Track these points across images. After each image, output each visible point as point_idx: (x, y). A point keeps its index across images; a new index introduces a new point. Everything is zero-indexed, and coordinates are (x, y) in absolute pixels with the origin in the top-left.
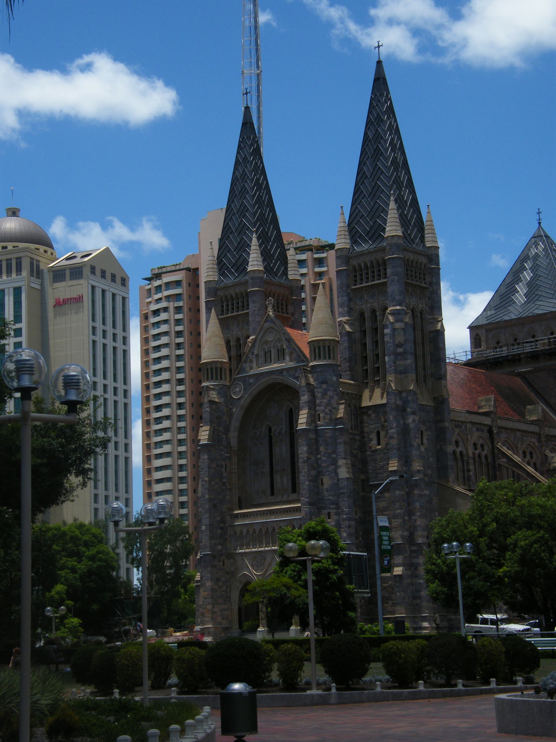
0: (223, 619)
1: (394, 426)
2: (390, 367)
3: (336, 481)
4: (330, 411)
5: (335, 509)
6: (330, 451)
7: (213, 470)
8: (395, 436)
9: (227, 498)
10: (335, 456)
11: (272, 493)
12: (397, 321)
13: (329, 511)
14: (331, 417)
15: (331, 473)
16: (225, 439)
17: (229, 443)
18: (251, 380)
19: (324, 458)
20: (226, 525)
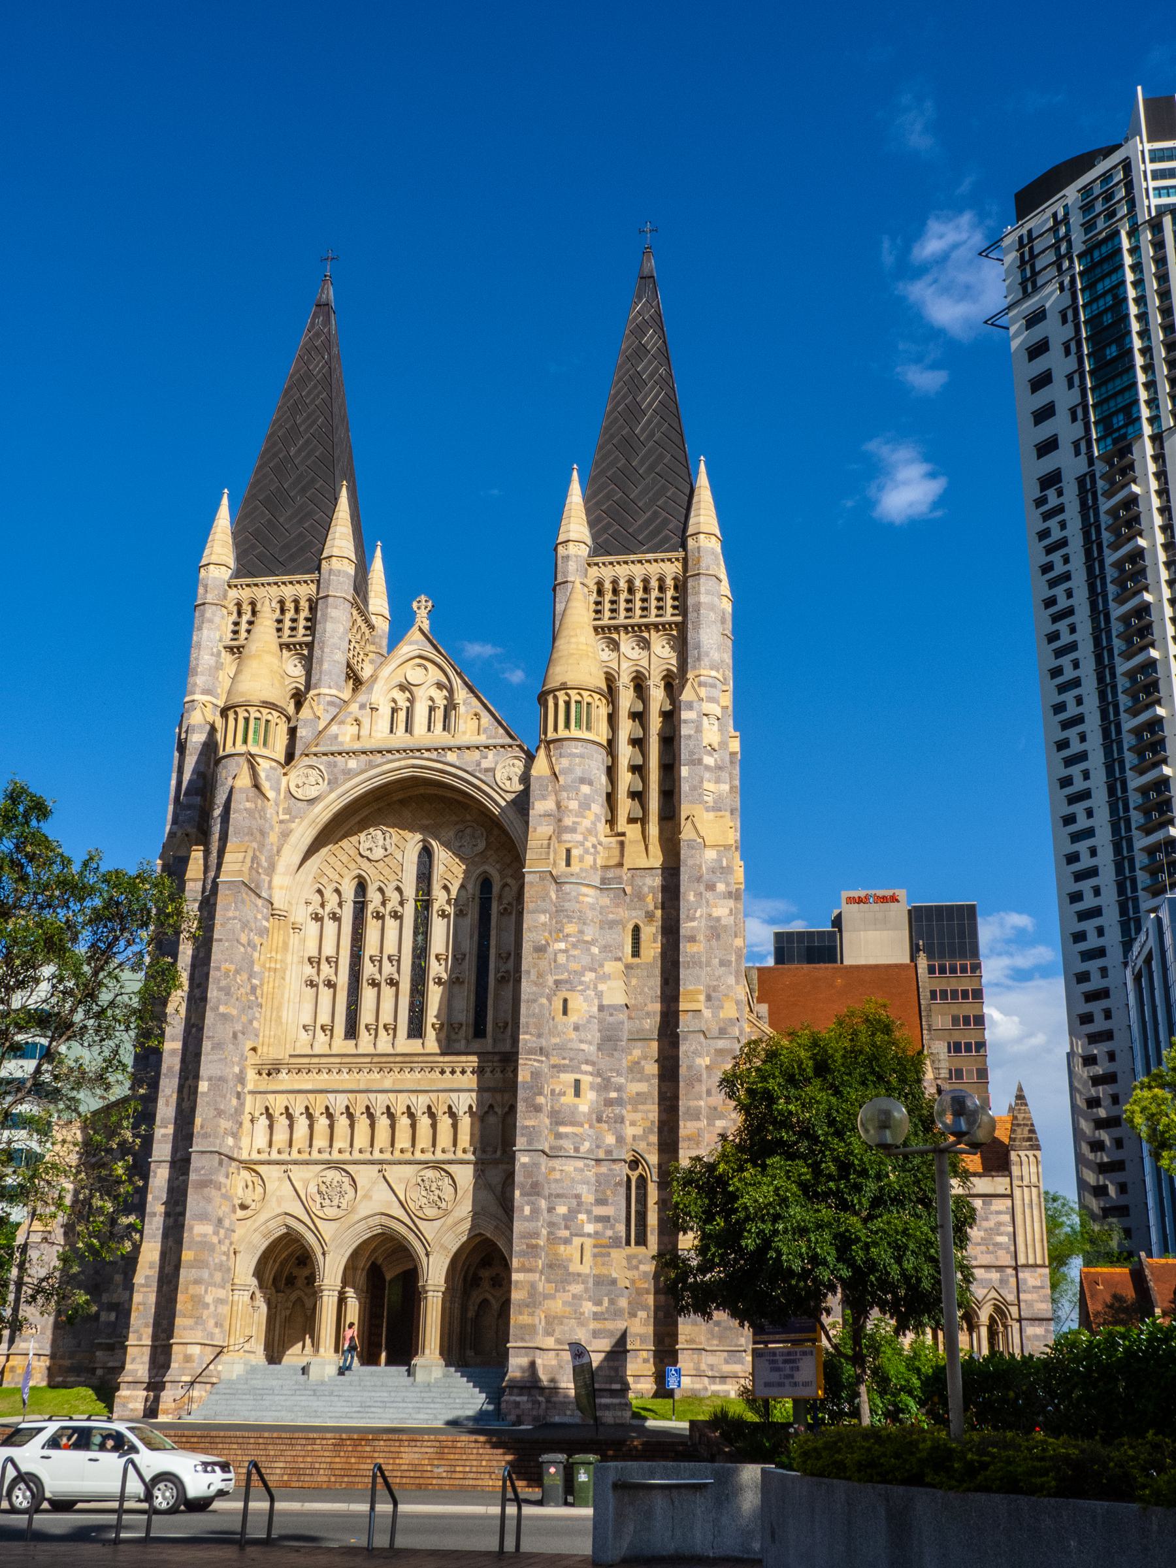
0: (216, 1325)
1: (698, 914)
2: (693, 788)
3: (595, 1009)
4: (594, 846)
5: (591, 1074)
6: (588, 938)
7: (242, 949)
8: (701, 937)
9: (255, 1024)
10: (595, 950)
11: (352, 1032)
12: (712, 700)
13: (578, 1076)
14: (595, 860)
15: (588, 988)
16: (266, 885)
17: (271, 896)
18: (352, 764)
19: (576, 952)
20: (246, 1090)
